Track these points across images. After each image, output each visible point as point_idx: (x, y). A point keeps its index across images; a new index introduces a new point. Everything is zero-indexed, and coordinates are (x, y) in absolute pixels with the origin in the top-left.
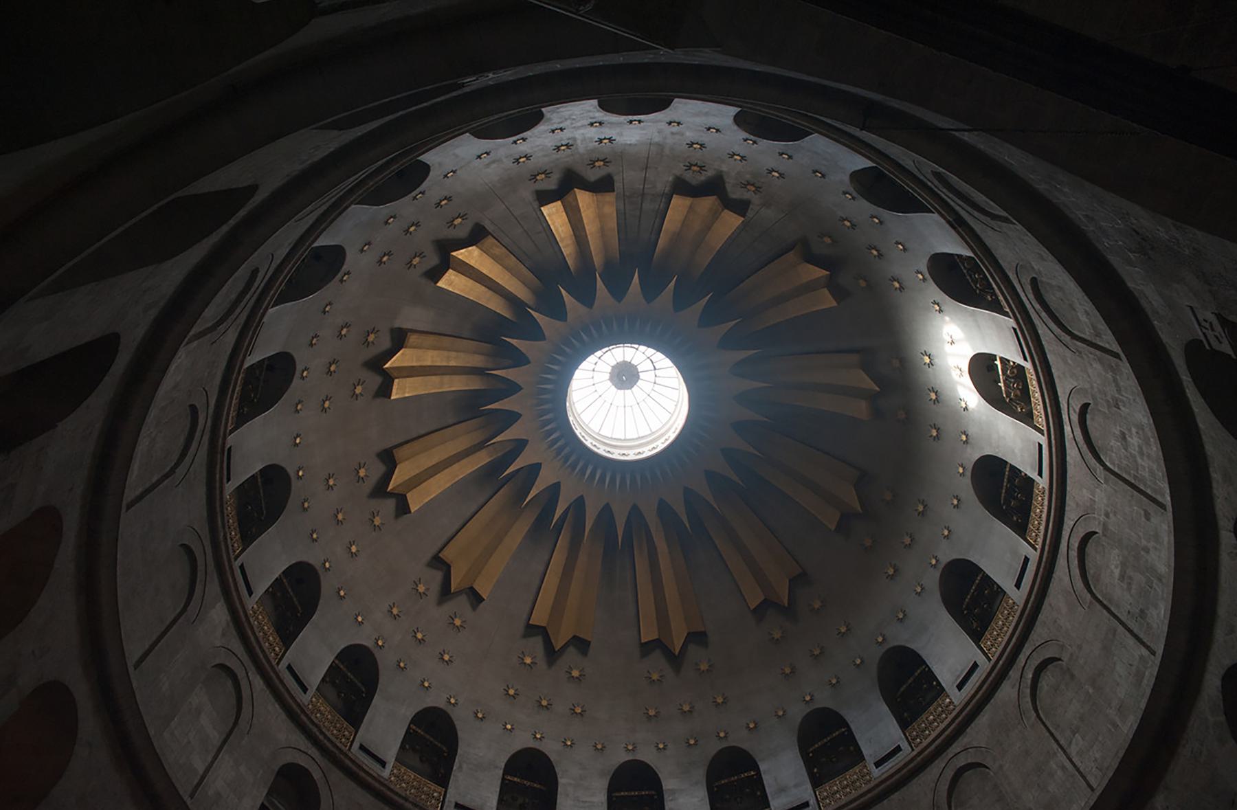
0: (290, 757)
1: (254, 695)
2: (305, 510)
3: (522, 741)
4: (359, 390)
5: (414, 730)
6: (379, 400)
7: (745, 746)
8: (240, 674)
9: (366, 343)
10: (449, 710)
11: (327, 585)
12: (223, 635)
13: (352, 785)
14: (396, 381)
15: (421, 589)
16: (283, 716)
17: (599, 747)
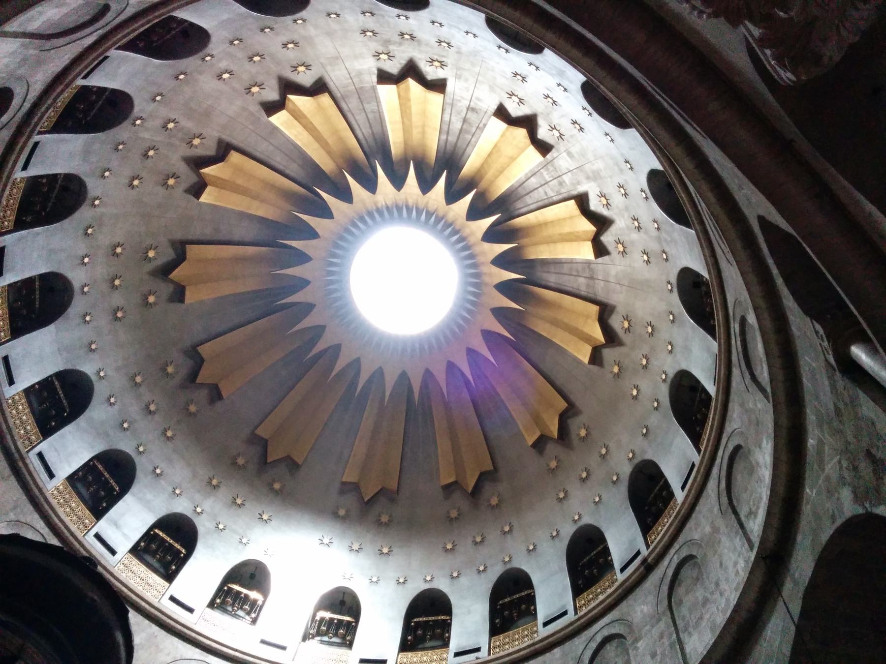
0: (19, 91)
3: (77, 277)
7: (139, 474)
10: (88, 202)
11: (190, 63)
15: (196, 142)
17: (93, 347)
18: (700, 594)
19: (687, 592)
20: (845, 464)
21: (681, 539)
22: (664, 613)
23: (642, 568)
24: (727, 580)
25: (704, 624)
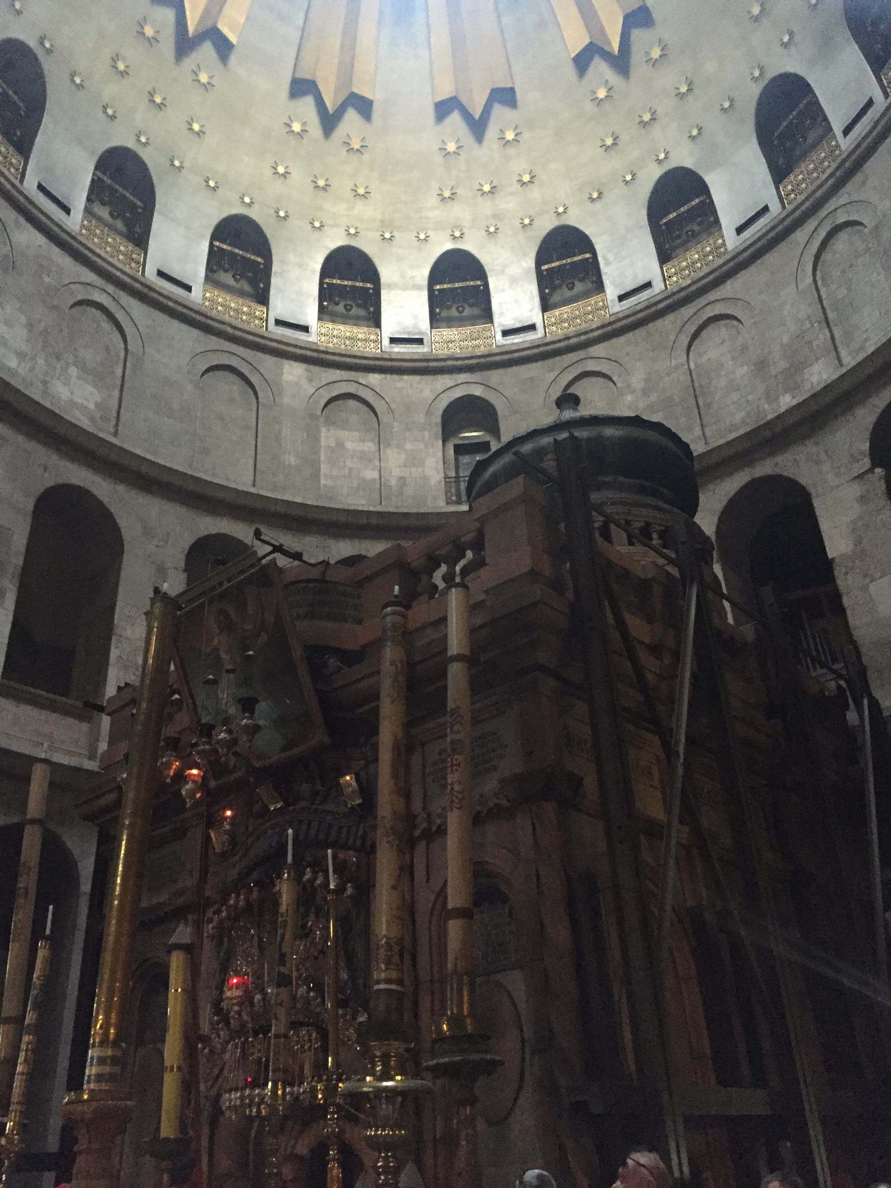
1: (378, 391)
2: (286, 217)
4: (204, 78)
5: (547, 270)
6: (233, 59)
8: (351, 388)
9: (152, 41)
12: (310, 381)
13: (514, 369)
14: (220, 26)
16: (416, 378)
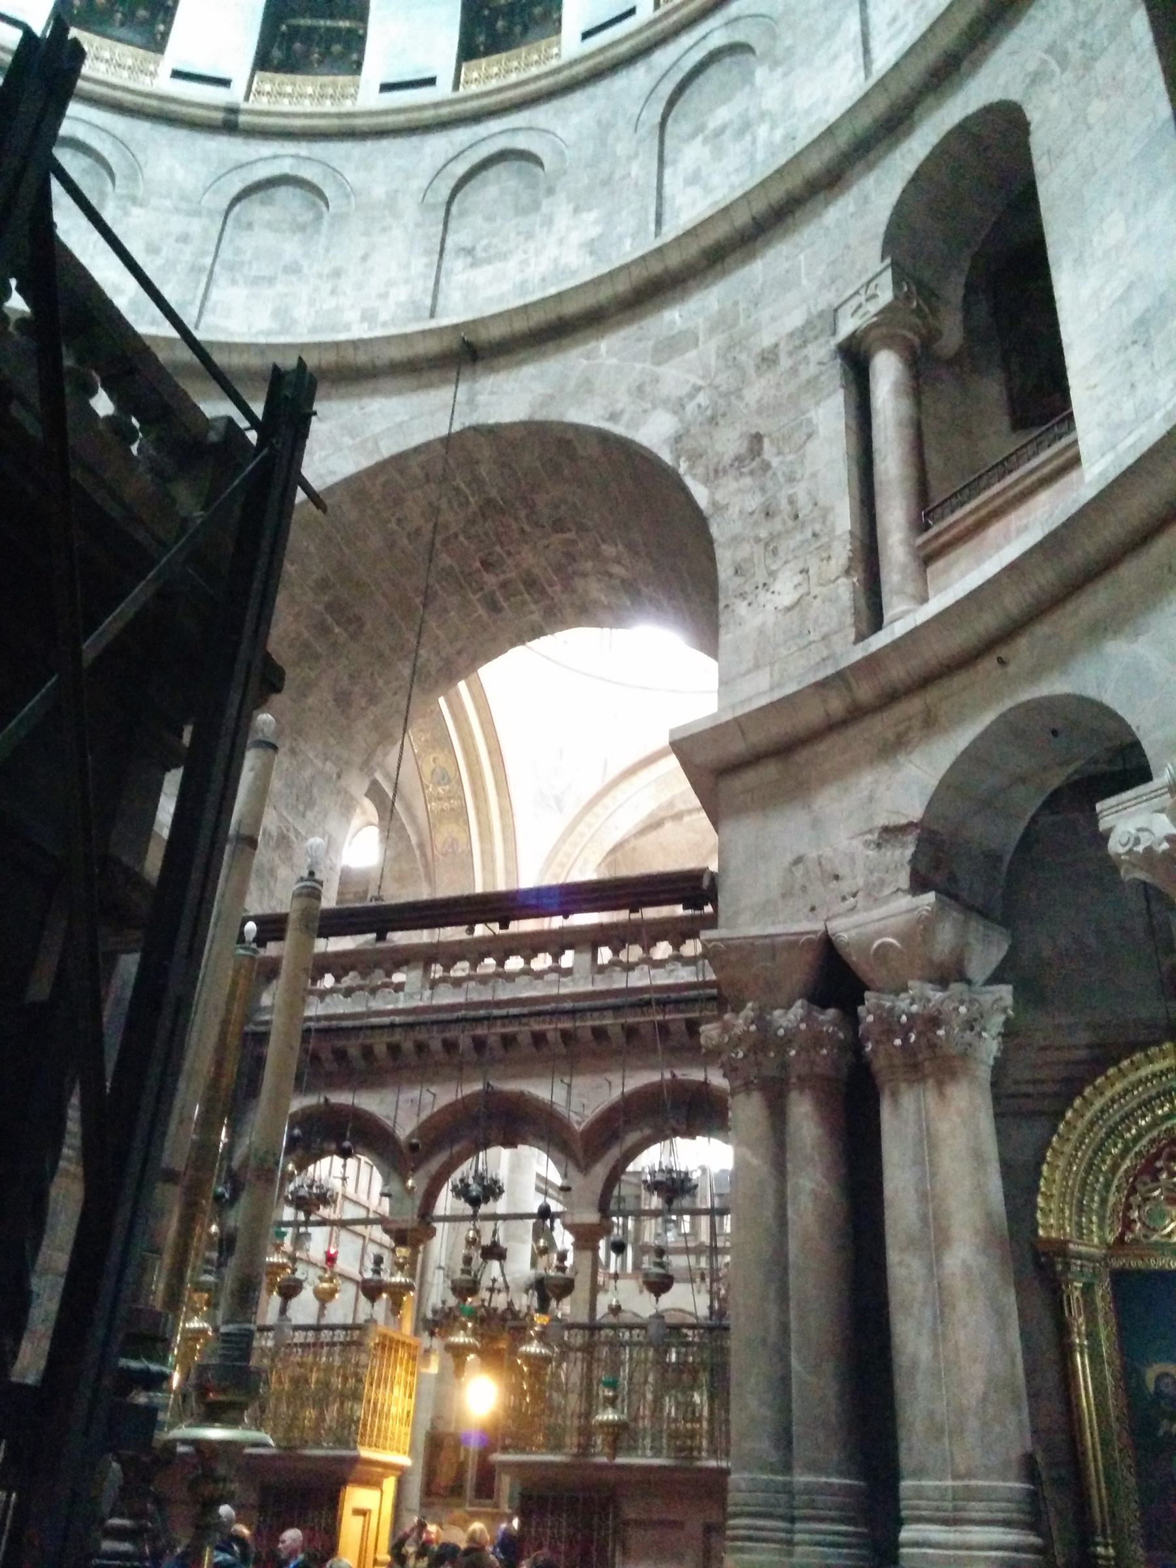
18: (291, 248)
19: (269, 226)
20: (702, 399)
21: (319, 149)
22: (211, 213)
23: (220, 116)
24: (359, 286)
25: (269, 292)
